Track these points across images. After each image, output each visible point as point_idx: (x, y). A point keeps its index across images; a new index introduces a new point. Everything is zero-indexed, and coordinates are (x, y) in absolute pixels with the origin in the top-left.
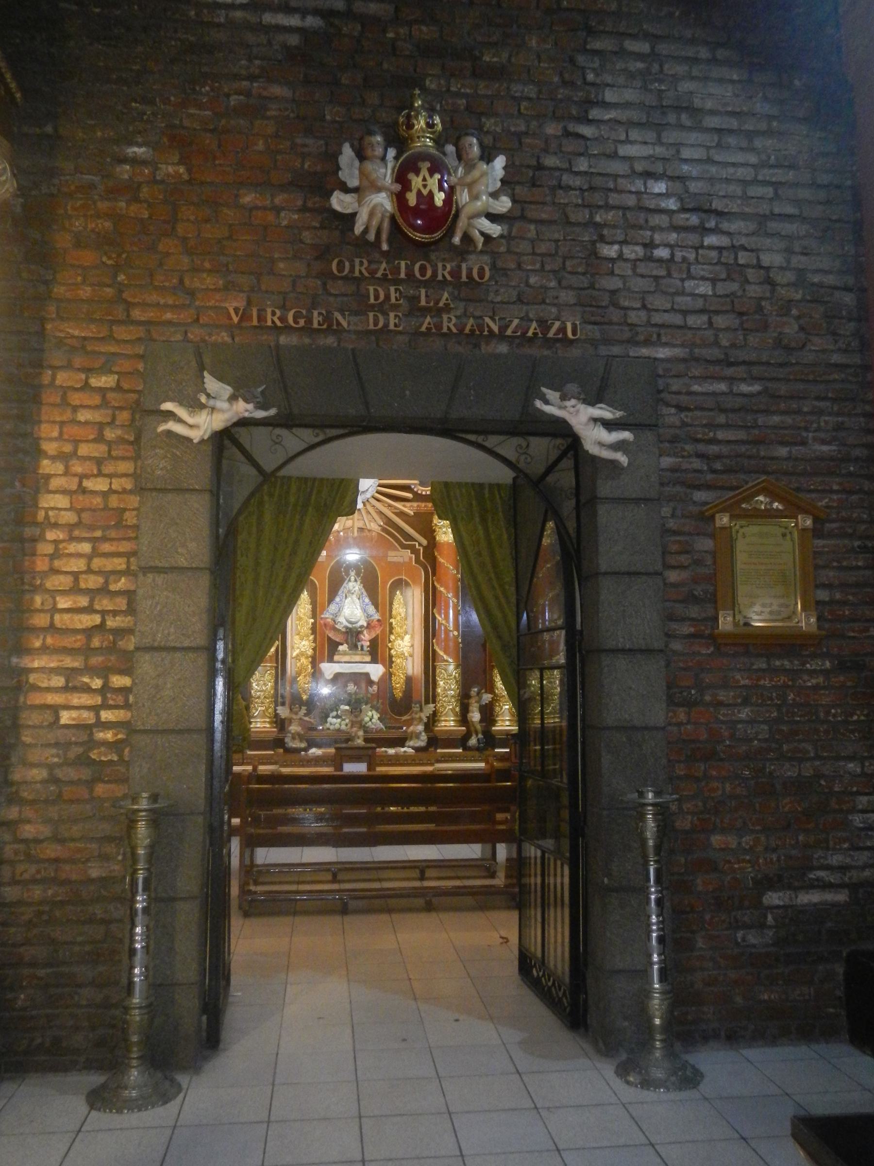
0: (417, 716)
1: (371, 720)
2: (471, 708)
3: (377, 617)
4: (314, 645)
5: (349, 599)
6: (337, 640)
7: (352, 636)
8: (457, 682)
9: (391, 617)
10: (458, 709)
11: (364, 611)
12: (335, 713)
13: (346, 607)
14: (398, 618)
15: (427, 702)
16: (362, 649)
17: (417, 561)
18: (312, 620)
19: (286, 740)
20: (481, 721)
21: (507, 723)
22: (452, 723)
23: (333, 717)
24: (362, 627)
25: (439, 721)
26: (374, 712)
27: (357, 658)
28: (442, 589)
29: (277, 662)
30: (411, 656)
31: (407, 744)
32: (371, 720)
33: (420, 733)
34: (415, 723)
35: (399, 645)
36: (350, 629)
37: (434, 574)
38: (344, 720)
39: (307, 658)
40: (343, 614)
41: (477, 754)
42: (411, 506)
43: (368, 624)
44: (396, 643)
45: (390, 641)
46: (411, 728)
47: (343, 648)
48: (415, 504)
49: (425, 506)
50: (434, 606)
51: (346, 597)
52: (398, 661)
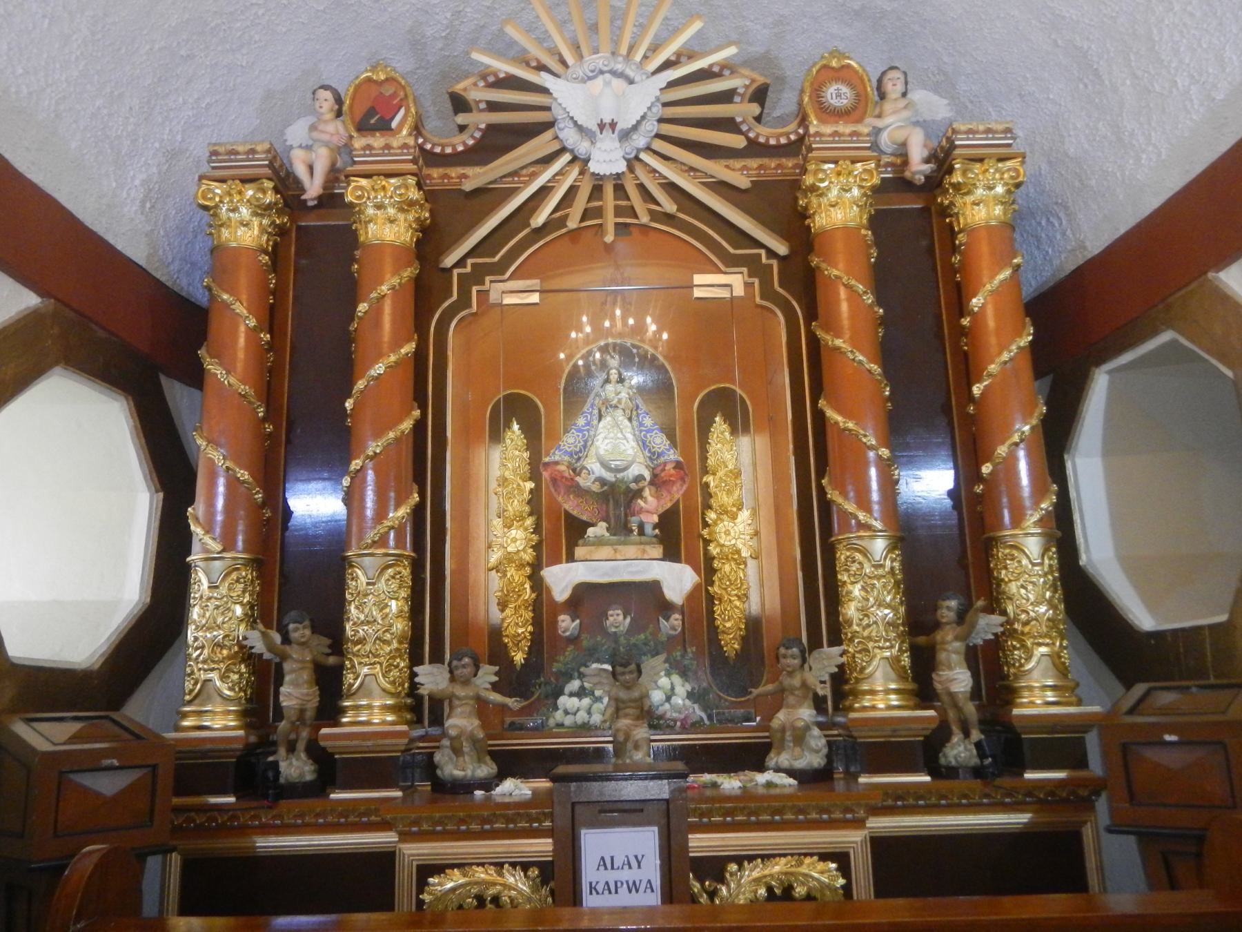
0: (796, 682)
1: (668, 699)
2: (942, 656)
3: (673, 456)
4: (535, 537)
5: (607, 420)
6: (584, 518)
7: (617, 504)
8: (897, 583)
9: (705, 471)
10: (906, 660)
11: (644, 444)
12: (575, 685)
13: (600, 437)
14: (720, 474)
15: (815, 643)
16: (641, 532)
17: (767, 293)
18: (530, 485)
19: (438, 757)
20: (975, 694)
21: (1051, 696)
22: (894, 700)
23: (571, 695)
24: (639, 478)
25: (856, 694)
26: (676, 679)
27: (631, 551)
28: (839, 342)
29: (418, 545)
30: (756, 557)
31: (772, 760)
32: (668, 699)
33: (807, 728)
34: (791, 700)
35: (727, 533)
36: (613, 486)
37: (812, 314)
38: (599, 699)
39: (521, 566)
40: (593, 451)
41: (977, 784)
42: (744, 168)
43: (655, 475)
44: (720, 528)
45: (706, 525)
46: (781, 717)
47: (598, 530)
48: (754, 163)
49: (779, 166)
50: (817, 391)
51: (600, 417)
52: (727, 568)
